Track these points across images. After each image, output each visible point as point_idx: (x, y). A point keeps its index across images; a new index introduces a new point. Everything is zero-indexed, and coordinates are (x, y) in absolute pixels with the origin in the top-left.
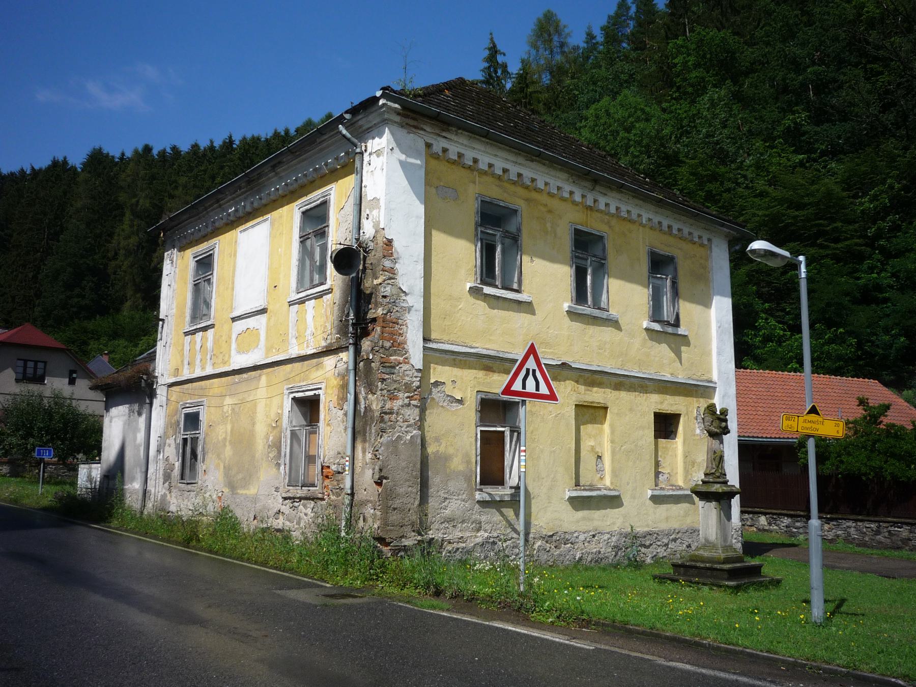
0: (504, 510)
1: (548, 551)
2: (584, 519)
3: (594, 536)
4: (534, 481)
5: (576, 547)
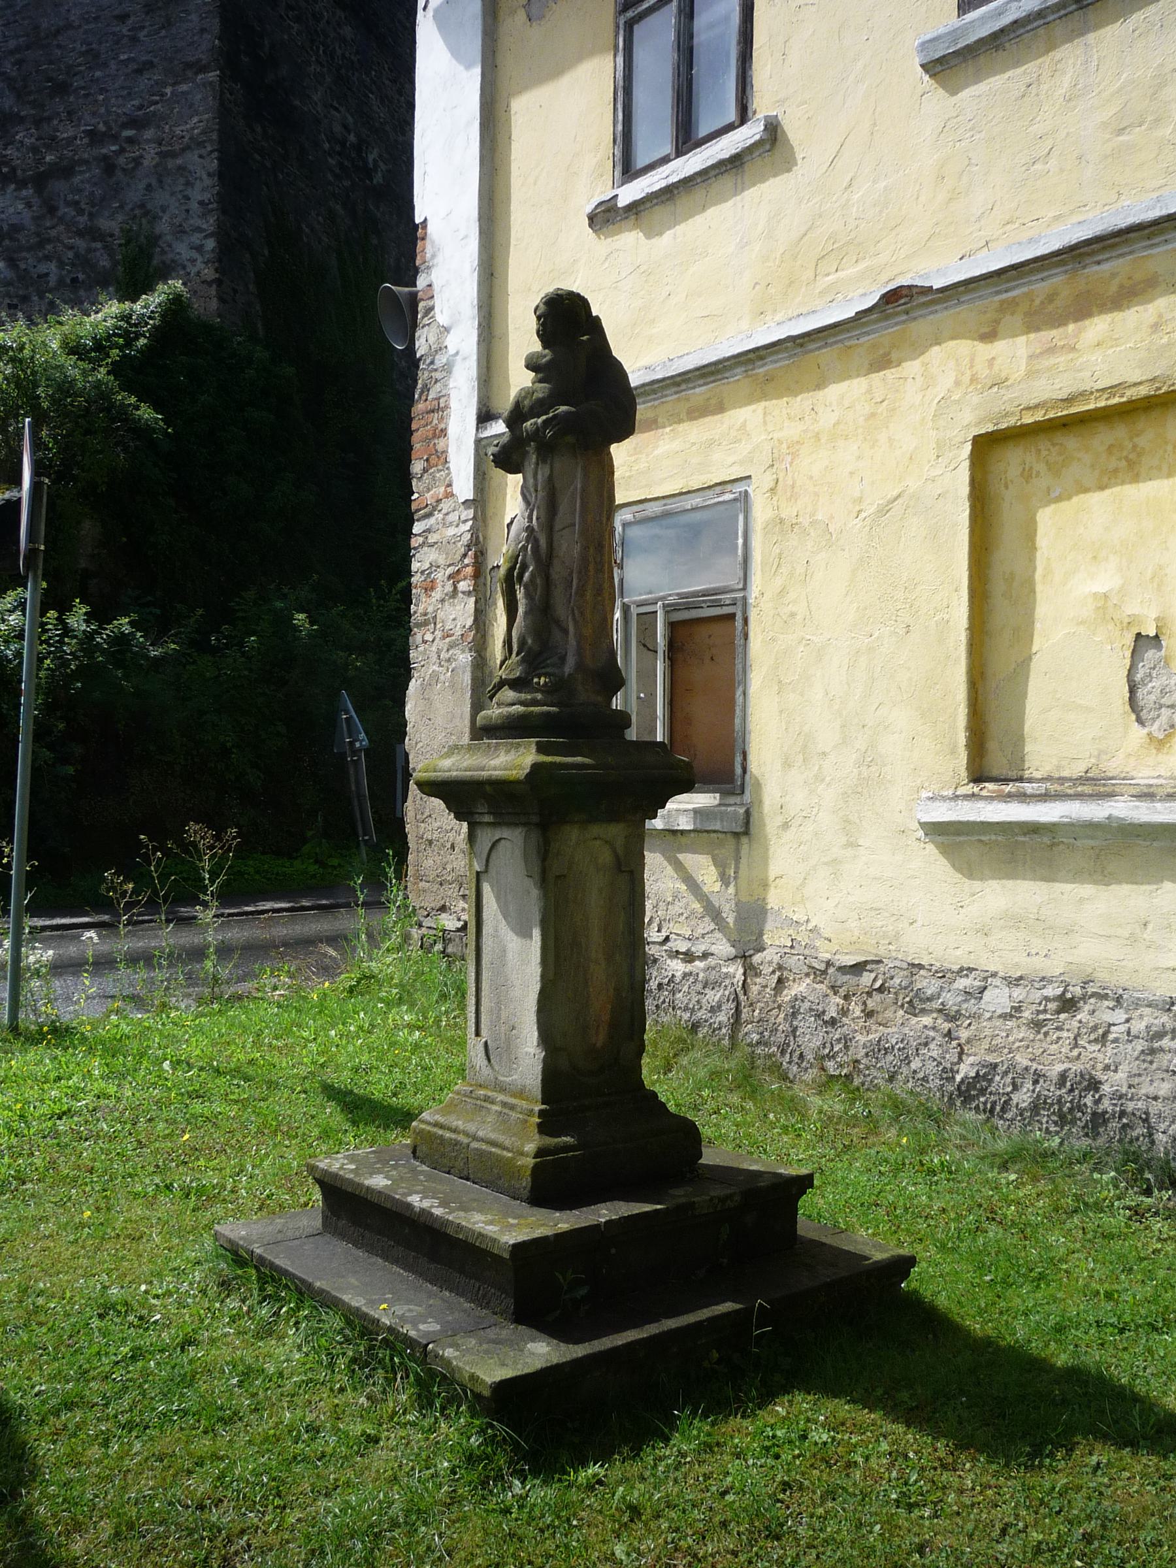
0: (687, 859)
1: (833, 1022)
2: (1014, 921)
3: (1068, 1004)
4: (787, 764)
5: (964, 1034)
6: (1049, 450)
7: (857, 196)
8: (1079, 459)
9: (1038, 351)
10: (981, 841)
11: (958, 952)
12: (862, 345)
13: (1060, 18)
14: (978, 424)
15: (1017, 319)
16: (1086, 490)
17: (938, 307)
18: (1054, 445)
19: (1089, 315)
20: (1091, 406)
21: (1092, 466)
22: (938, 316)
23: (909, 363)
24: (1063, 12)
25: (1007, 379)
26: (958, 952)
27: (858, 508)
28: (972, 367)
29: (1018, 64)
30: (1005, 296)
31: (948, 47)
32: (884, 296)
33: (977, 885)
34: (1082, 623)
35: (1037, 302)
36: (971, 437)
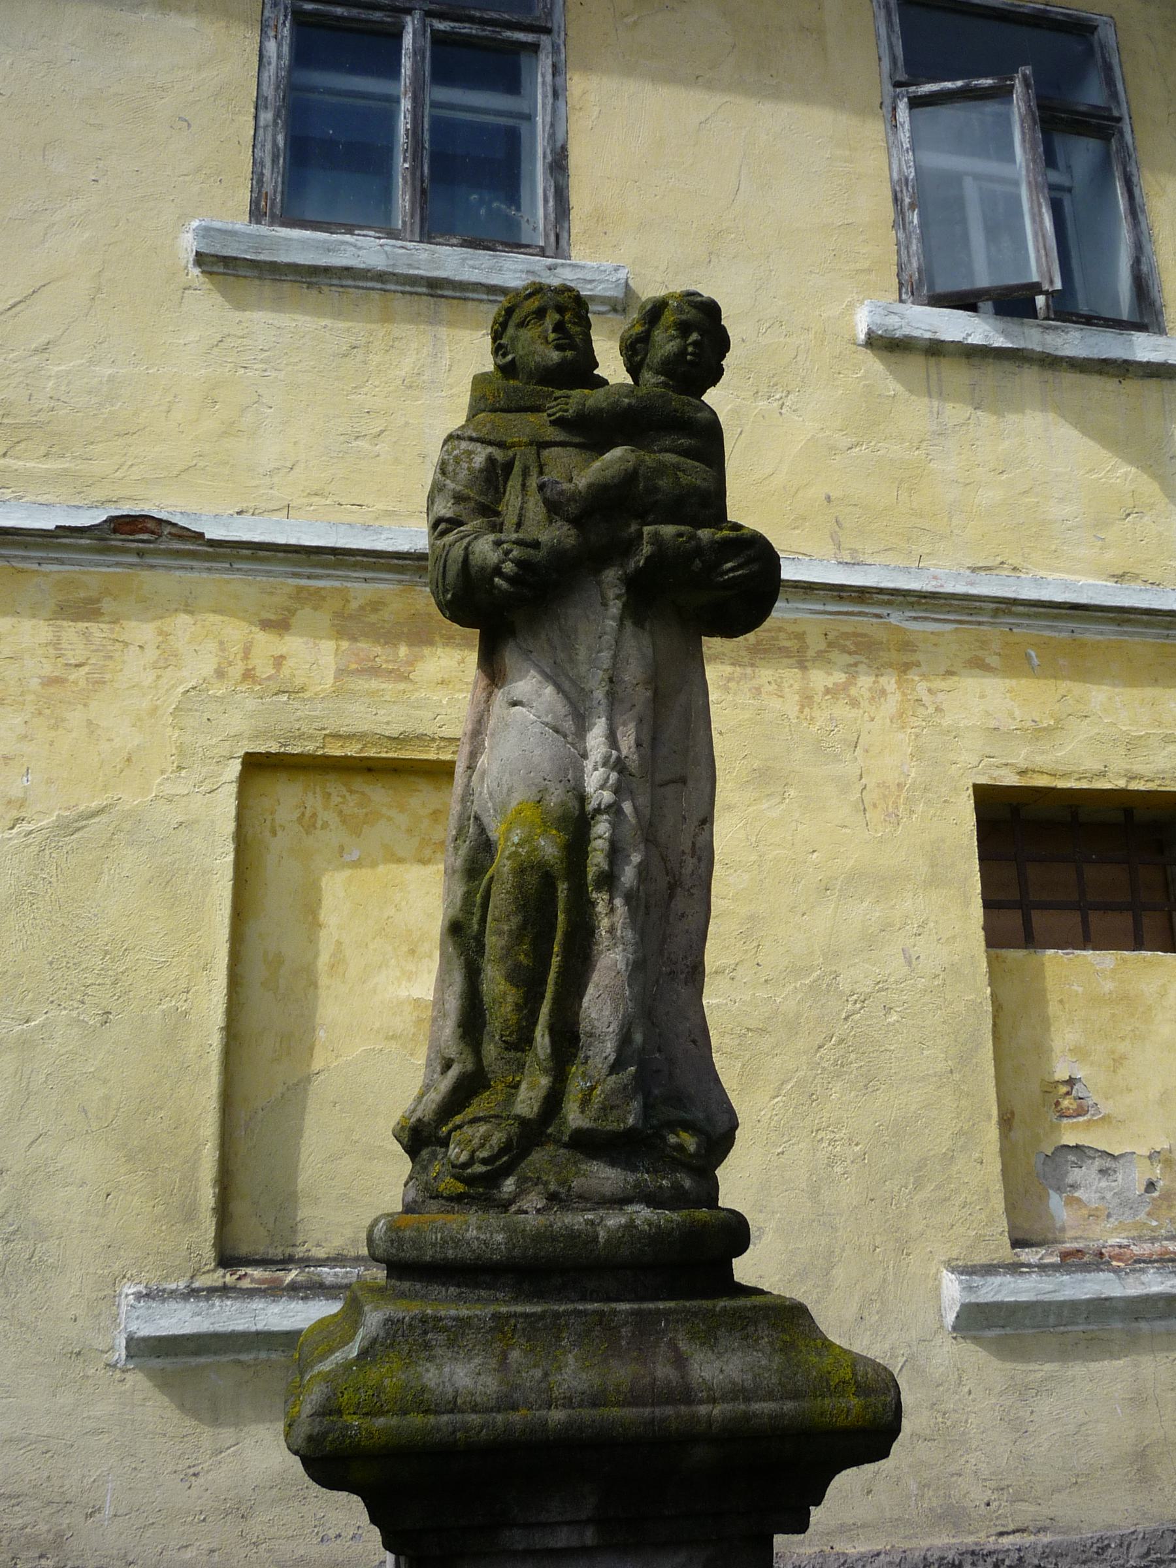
6: (344, 797)
7: (56, 369)
8: (389, 819)
9: (354, 666)
10: (240, 1362)
11: (188, 1554)
12: (46, 575)
13: (403, 293)
14: (255, 737)
15: (324, 618)
16: (400, 861)
17: (195, 564)
18: (351, 792)
19: (431, 643)
20: (432, 756)
21: (410, 831)
22: (195, 575)
23: (134, 624)
24: (408, 289)
25: (303, 690)
26: (188, 1554)
27: (15, 814)
28: (246, 657)
29: (338, 315)
30: (304, 582)
31: (246, 251)
32: (112, 519)
33: (227, 1434)
34: (393, 1037)
35: (354, 605)
36: (242, 753)
